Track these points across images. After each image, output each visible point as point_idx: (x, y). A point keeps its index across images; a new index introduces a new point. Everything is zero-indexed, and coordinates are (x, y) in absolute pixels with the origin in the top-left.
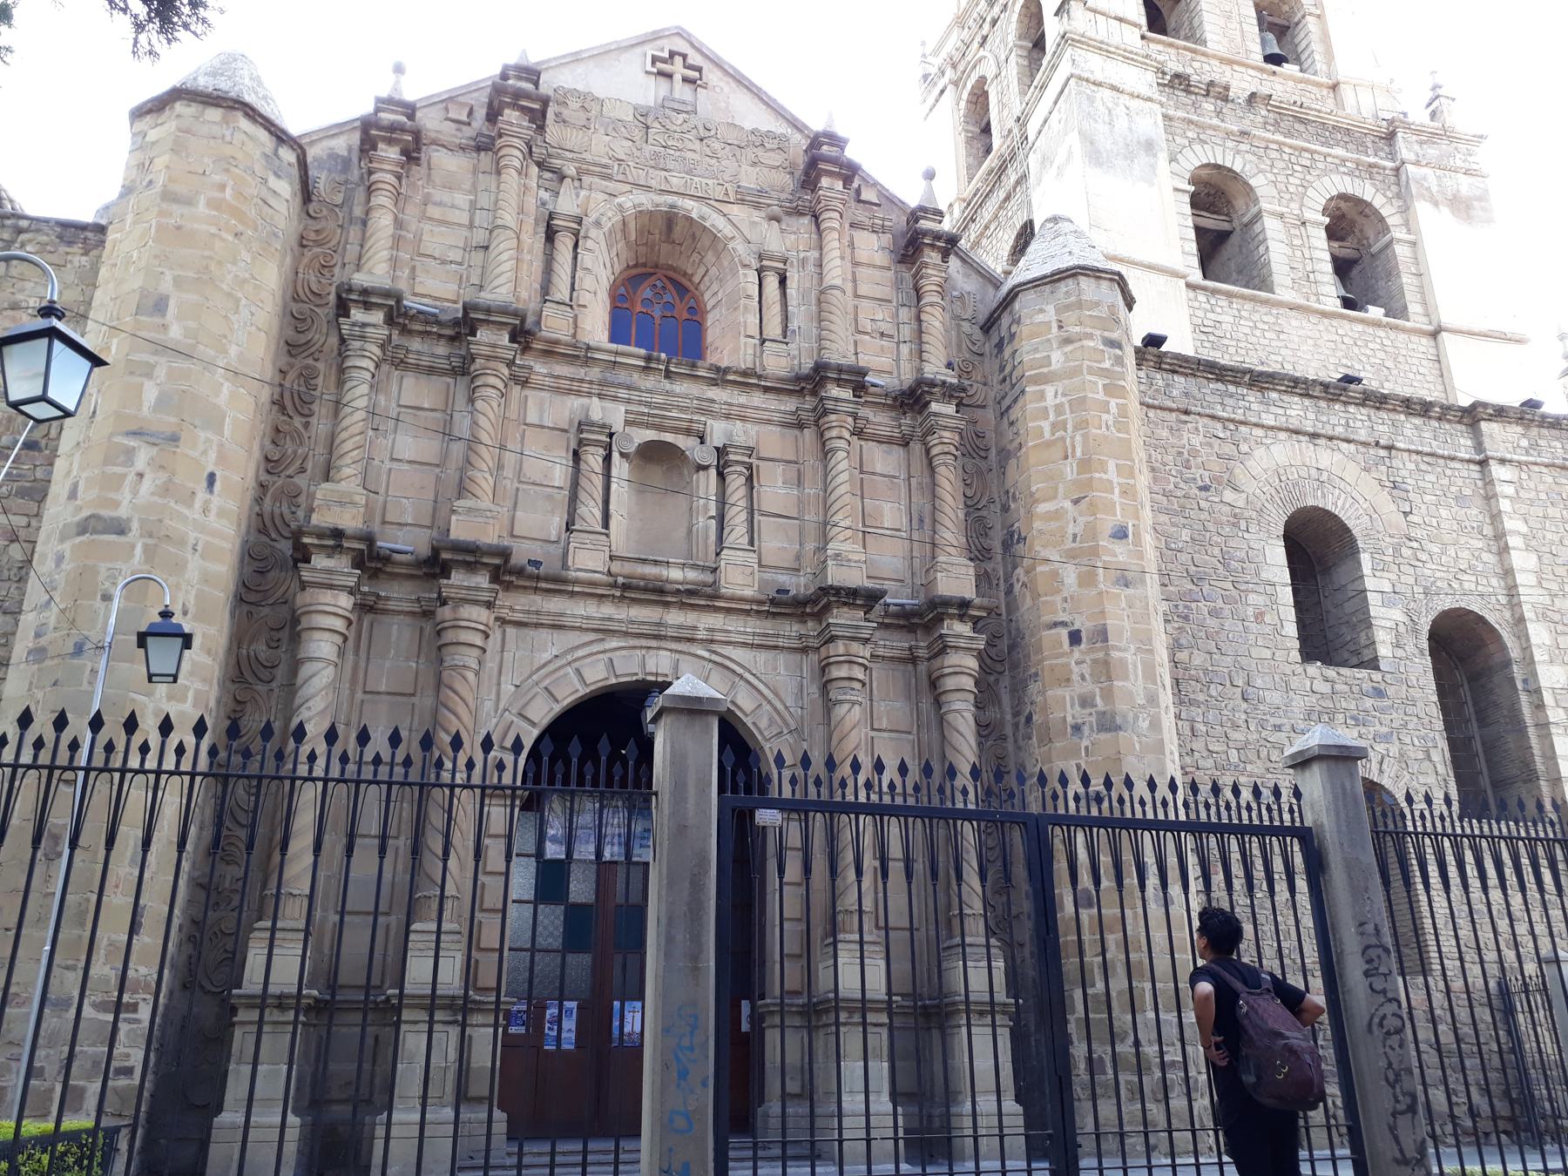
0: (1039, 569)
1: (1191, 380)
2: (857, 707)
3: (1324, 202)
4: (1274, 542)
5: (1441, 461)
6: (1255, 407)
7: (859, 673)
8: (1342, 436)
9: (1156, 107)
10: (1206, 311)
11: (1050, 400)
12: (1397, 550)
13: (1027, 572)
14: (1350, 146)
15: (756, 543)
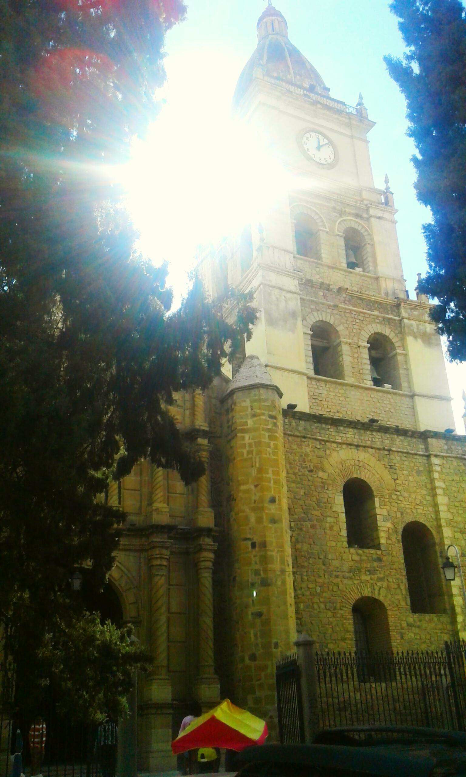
0: (241, 514)
1: (308, 423)
2: (163, 578)
3: (368, 336)
4: (339, 494)
5: (411, 456)
6: (333, 434)
7: (165, 563)
8: (370, 446)
9: (298, 297)
10: (315, 388)
11: (247, 441)
12: (390, 496)
13: (236, 514)
14: (381, 310)
15: (122, 503)
